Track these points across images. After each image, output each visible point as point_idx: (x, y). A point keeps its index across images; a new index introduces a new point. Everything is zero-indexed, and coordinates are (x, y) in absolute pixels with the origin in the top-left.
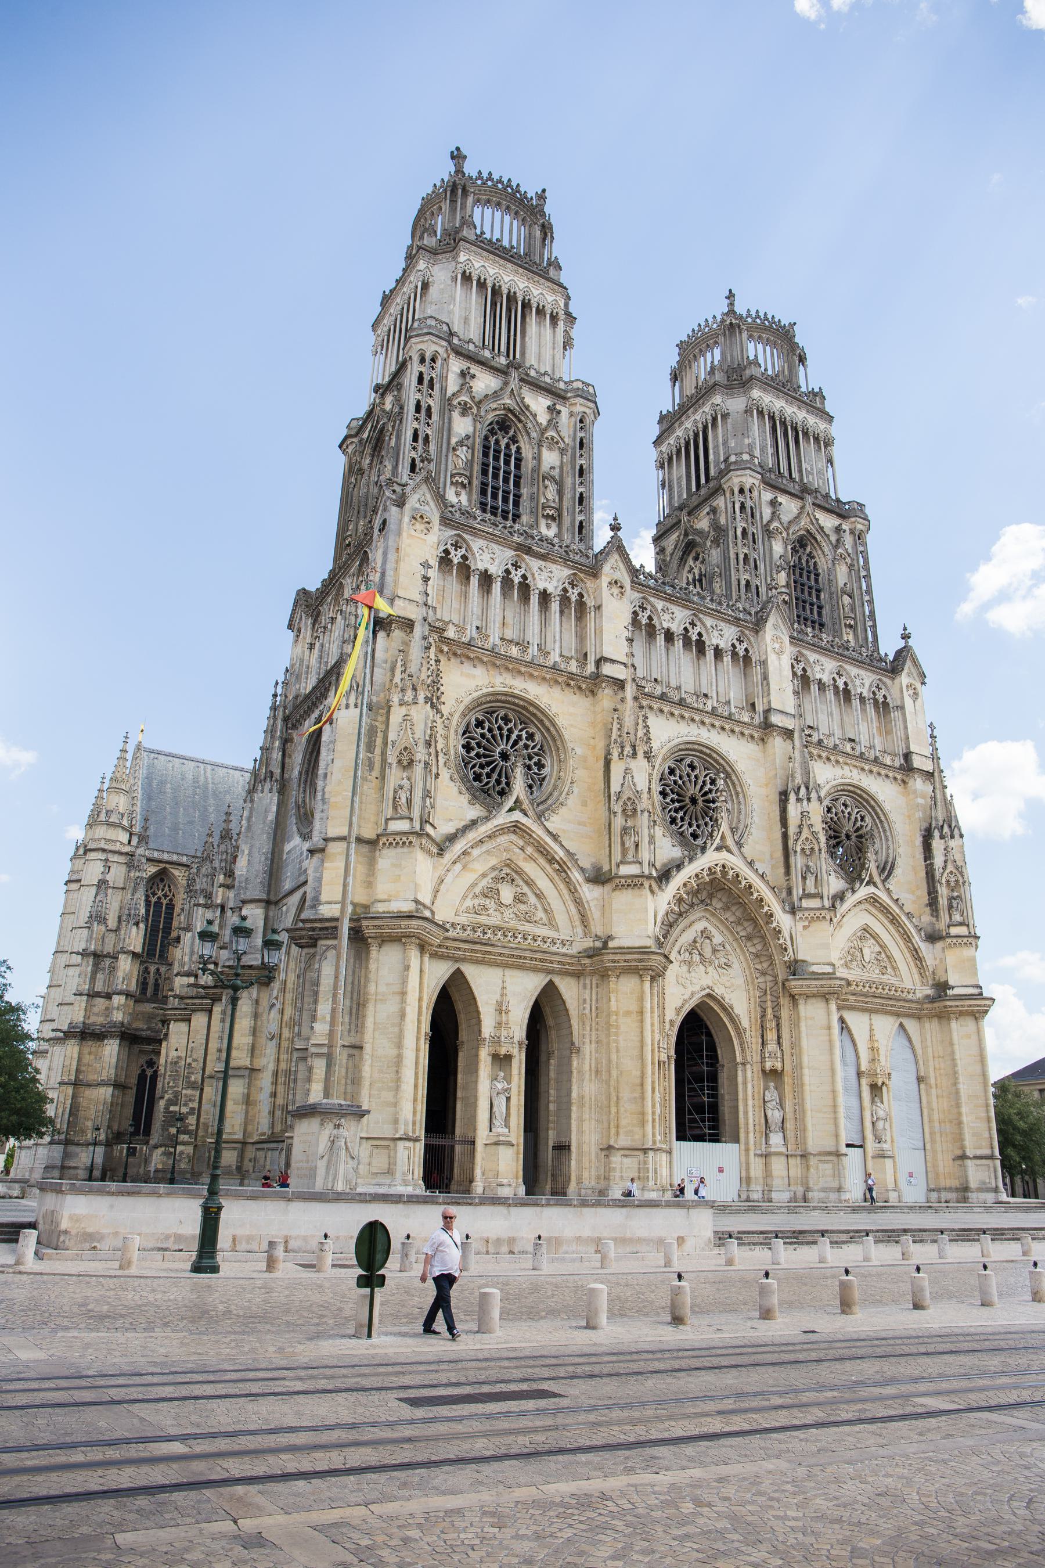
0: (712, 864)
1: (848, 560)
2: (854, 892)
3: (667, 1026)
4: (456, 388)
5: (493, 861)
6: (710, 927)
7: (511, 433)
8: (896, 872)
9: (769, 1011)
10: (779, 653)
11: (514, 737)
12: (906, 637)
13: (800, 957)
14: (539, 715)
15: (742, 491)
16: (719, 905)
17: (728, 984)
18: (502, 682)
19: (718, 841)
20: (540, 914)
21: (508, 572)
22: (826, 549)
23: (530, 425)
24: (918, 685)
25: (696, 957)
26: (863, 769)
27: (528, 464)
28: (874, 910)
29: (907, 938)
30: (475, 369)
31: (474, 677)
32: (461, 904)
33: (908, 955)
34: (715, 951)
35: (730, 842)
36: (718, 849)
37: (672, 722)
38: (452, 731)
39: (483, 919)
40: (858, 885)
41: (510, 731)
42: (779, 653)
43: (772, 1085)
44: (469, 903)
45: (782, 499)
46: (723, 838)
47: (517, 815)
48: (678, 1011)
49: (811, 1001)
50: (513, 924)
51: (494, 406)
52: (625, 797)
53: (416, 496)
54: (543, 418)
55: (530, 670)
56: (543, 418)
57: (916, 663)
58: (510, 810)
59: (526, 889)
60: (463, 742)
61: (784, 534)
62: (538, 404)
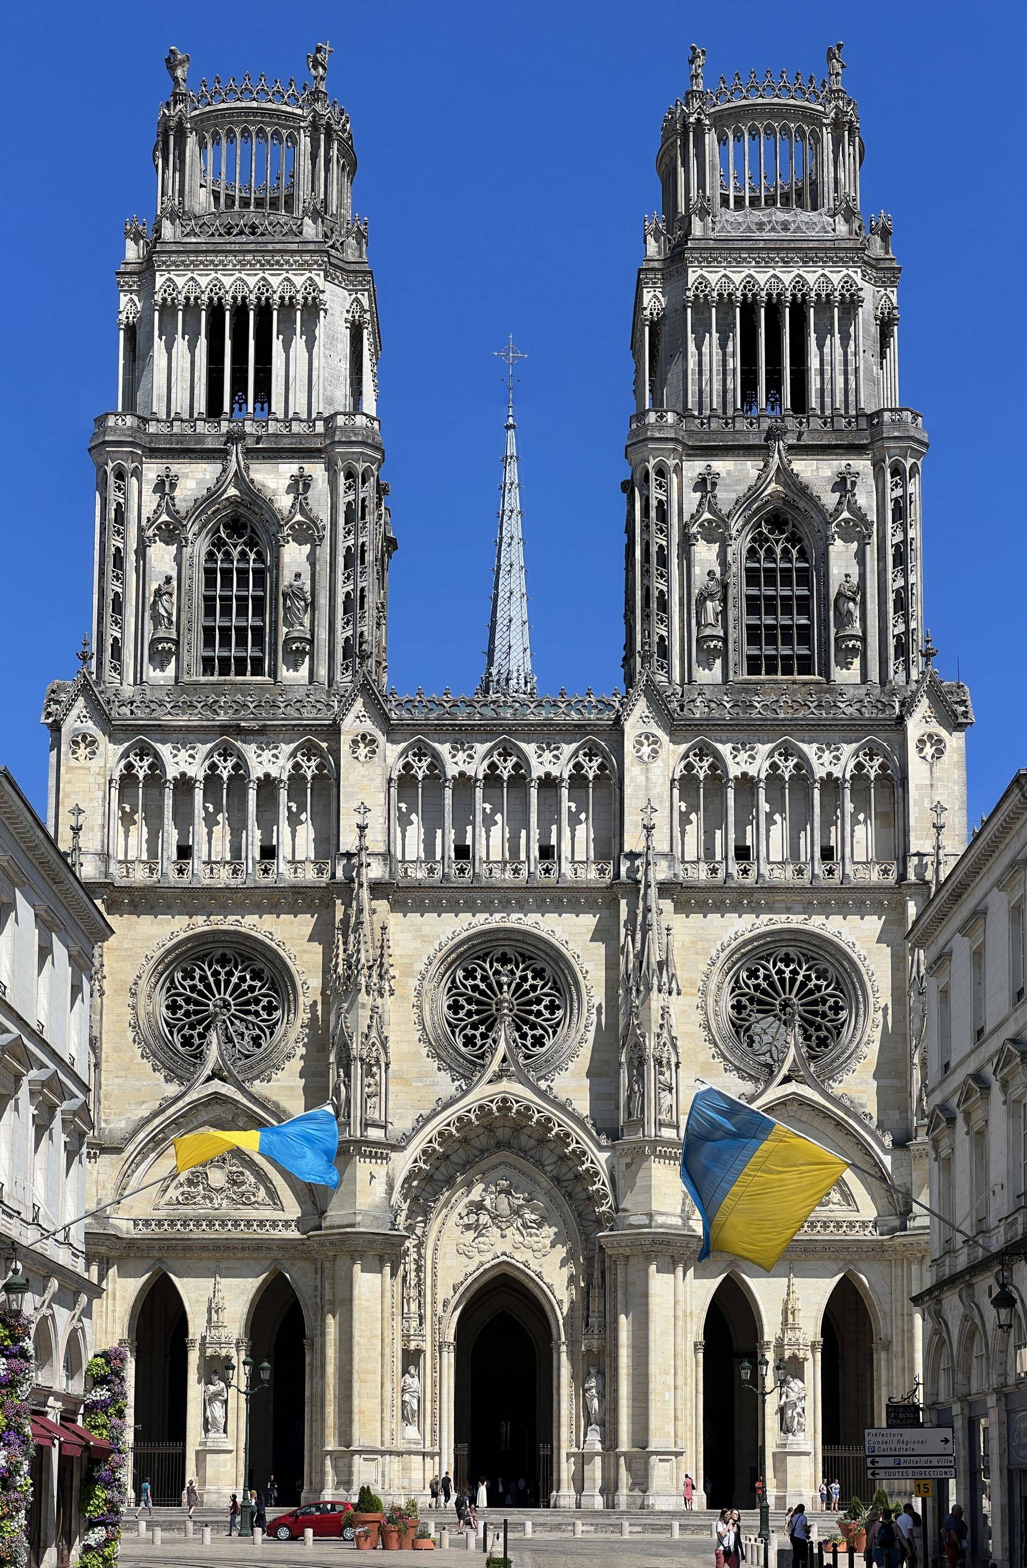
9: (597, 1274)
11: (234, 980)
17: (535, 1247)
19: (495, 1066)
20: (262, 1193)
21: (213, 767)
25: (484, 1219)
38: (142, 999)
39: (188, 1211)
43: (593, 1371)
44: (173, 1193)
45: (721, 466)
47: (216, 1086)
49: (632, 1262)
53: (74, 713)
54: (284, 502)
58: (209, 1079)
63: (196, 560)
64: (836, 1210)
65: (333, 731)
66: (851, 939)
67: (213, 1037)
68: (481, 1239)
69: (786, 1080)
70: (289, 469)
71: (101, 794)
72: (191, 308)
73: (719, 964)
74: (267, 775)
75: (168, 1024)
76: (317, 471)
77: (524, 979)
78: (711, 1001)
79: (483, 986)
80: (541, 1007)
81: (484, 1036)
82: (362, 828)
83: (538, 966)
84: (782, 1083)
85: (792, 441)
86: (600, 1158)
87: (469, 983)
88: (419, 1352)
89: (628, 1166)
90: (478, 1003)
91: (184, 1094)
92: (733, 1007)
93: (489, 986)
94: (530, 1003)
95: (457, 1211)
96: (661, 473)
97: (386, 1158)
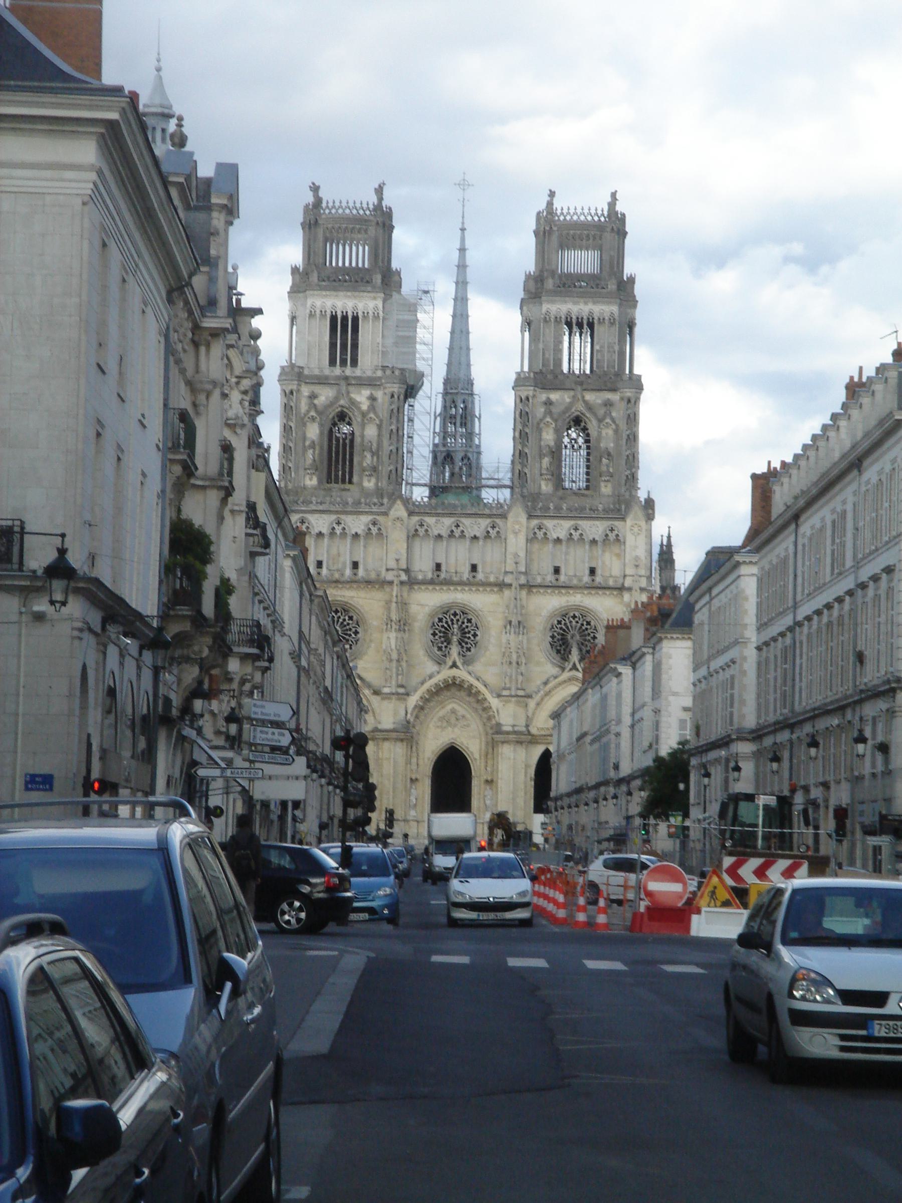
1: (614, 426)
2: (556, 677)
3: (426, 760)
4: (307, 408)
7: (347, 419)
10: (516, 533)
11: (341, 620)
19: (450, 663)
21: (333, 529)
24: (643, 523)
25: (445, 724)
27: (358, 440)
30: (317, 389)
34: (457, 719)
36: (451, 667)
41: (339, 617)
42: (516, 533)
45: (554, 396)
48: (433, 752)
54: (364, 407)
56: (364, 407)
61: (554, 425)
62: (362, 397)
65: (386, 514)
69: (571, 670)
70: (366, 392)
74: (356, 533)
76: (379, 394)
77: (463, 623)
81: (446, 647)
82: (397, 560)
85: (584, 387)
86: (494, 702)
87: (440, 624)
88: (417, 779)
90: (444, 633)
94: (465, 633)
96: (528, 399)
97: (405, 700)
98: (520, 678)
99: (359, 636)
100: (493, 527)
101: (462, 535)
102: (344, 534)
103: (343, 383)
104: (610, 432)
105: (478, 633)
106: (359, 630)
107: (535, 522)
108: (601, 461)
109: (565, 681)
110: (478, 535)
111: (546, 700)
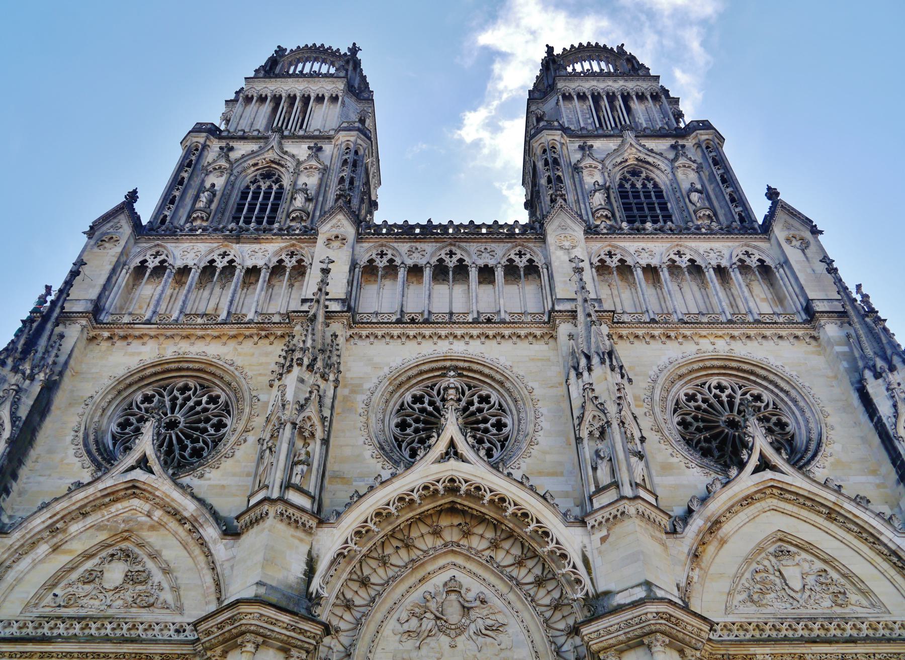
0: (431, 479)
1: (694, 166)
5: (102, 536)
6: (464, 579)
8: (826, 449)
11: (191, 403)
12: (772, 194)
13: (601, 588)
14: (218, 372)
15: (545, 151)
16: (484, 544)
18: (171, 350)
19: (441, 446)
21: (213, 261)
22: (663, 166)
23: (289, 164)
25: (428, 623)
26: (732, 337)
28: (789, 507)
29: (874, 540)
31: (139, 354)
32: (38, 597)
33: (885, 566)
34: (466, 610)
35: (463, 447)
37: (411, 345)
40: (733, 472)
46: (452, 444)
50: (122, 613)
51: (251, 162)
52: (274, 419)
54: (302, 158)
55: (209, 332)
57: (793, 213)
59: (150, 565)
60: (121, 420)
61: (600, 166)
63: (237, 186)
64: (856, 606)
66: (779, 364)
67: (148, 429)
68: (424, 650)
69: (757, 470)
71: (109, 267)
72: (262, 99)
73: (661, 381)
75: (114, 437)
77: (471, 403)
78: (657, 410)
79: (430, 409)
80: (488, 425)
83: (484, 393)
84: (754, 473)
89: (603, 540)
90: (425, 422)
91: (99, 478)
92: (679, 424)
93: (437, 409)
95: (396, 617)
98: (639, 468)
99: (223, 431)
100: (520, 254)
101: (462, 270)
102: (230, 268)
103: (274, 139)
104: (693, 176)
105: (507, 420)
106: (228, 421)
107: (599, 247)
108: (690, 201)
109: (749, 500)
110: (491, 263)
111: (711, 549)
